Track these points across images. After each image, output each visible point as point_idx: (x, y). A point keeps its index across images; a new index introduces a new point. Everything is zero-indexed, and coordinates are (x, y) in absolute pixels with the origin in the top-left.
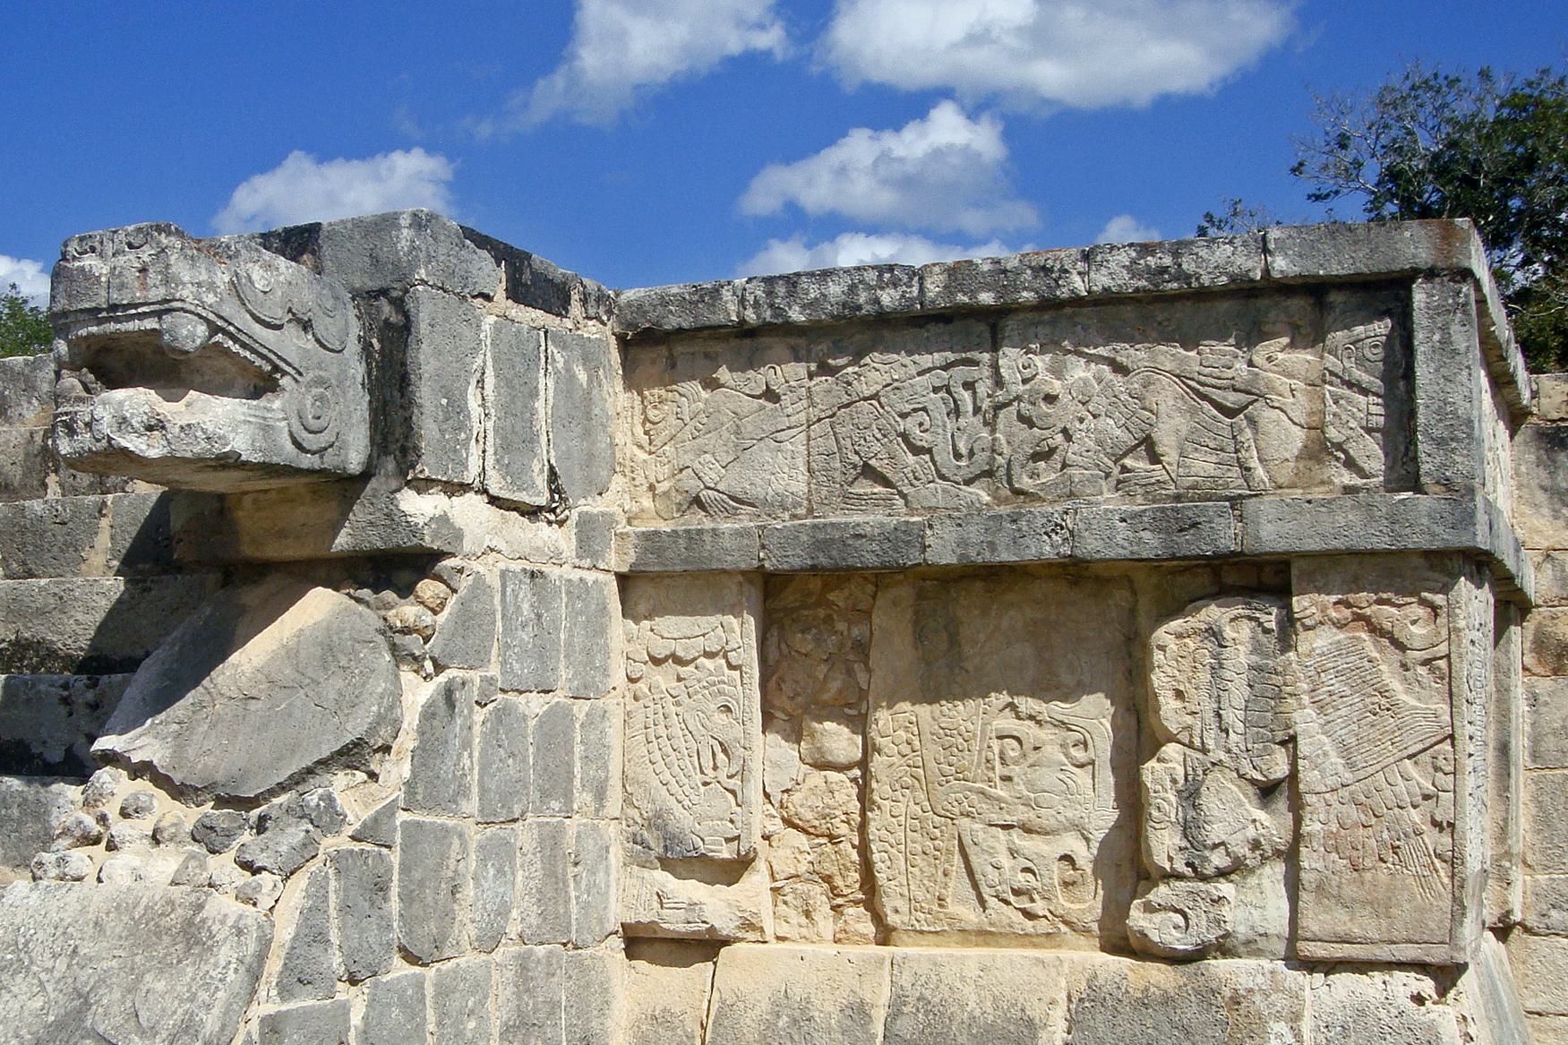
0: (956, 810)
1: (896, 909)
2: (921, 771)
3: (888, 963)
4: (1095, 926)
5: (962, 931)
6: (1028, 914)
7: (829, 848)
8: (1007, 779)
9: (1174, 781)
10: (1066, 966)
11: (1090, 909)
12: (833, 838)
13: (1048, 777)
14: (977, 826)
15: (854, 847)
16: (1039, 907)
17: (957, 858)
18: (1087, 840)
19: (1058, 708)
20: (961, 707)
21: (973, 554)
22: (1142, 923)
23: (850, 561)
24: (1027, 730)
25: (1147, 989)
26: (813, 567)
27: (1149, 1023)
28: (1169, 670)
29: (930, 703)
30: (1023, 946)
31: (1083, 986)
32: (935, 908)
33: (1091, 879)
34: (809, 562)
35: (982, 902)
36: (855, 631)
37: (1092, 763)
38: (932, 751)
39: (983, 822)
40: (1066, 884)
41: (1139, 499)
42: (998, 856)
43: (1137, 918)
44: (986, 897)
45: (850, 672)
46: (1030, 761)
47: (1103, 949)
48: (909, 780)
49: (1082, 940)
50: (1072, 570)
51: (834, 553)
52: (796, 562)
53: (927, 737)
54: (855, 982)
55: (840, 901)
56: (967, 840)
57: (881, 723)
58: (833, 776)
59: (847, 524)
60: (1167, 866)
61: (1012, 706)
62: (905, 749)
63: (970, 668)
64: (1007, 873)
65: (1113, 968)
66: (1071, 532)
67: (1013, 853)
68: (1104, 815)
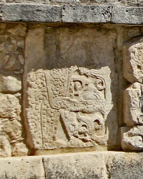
0: (59, 107)
1: (37, 143)
2: (46, 93)
3: (41, 161)
4: (106, 143)
5: (62, 148)
6: (84, 141)
7: (9, 122)
8: (77, 95)
9: (138, 94)
10: (104, 156)
11: (105, 137)
12: (10, 118)
13: (90, 94)
14: (67, 112)
15: (19, 121)
16: (88, 138)
17: (59, 124)
18: (103, 115)
19: (93, 71)
20: (61, 71)
21: (78, 19)
22: (129, 140)
23: (35, 19)
24: (83, 78)
25: (131, 161)
26: (21, 21)
27: (135, 172)
28: (136, 59)
29: (50, 69)
30: (83, 151)
31: (111, 162)
32: (52, 141)
33: (104, 127)
34: (20, 19)
35: (68, 138)
36: (19, 44)
37: (105, 89)
38: (50, 86)
39: (69, 110)
40: (96, 129)
41: (126, 5)
42: (73, 121)
43: (126, 138)
44: (70, 136)
45: (17, 59)
46: (84, 89)
47: (109, 150)
48: (42, 97)
49: (102, 148)
50: (98, 26)
51: (29, 16)
52: (15, 19)
53: (48, 81)
54: (31, 169)
55: (14, 141)
56: (63, 117)
57: (31, 77)
58: (10, 96)
59: (34, 6)
60: (137, 121)
61: (78, 71)
62: (41, 86)
63: (64, 58)
64: (77, 127)
65: (119, 155)
66: (111, 14)
67: (79, 120)
68: (108, 106)
